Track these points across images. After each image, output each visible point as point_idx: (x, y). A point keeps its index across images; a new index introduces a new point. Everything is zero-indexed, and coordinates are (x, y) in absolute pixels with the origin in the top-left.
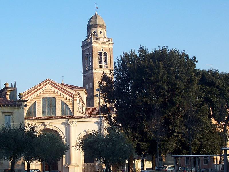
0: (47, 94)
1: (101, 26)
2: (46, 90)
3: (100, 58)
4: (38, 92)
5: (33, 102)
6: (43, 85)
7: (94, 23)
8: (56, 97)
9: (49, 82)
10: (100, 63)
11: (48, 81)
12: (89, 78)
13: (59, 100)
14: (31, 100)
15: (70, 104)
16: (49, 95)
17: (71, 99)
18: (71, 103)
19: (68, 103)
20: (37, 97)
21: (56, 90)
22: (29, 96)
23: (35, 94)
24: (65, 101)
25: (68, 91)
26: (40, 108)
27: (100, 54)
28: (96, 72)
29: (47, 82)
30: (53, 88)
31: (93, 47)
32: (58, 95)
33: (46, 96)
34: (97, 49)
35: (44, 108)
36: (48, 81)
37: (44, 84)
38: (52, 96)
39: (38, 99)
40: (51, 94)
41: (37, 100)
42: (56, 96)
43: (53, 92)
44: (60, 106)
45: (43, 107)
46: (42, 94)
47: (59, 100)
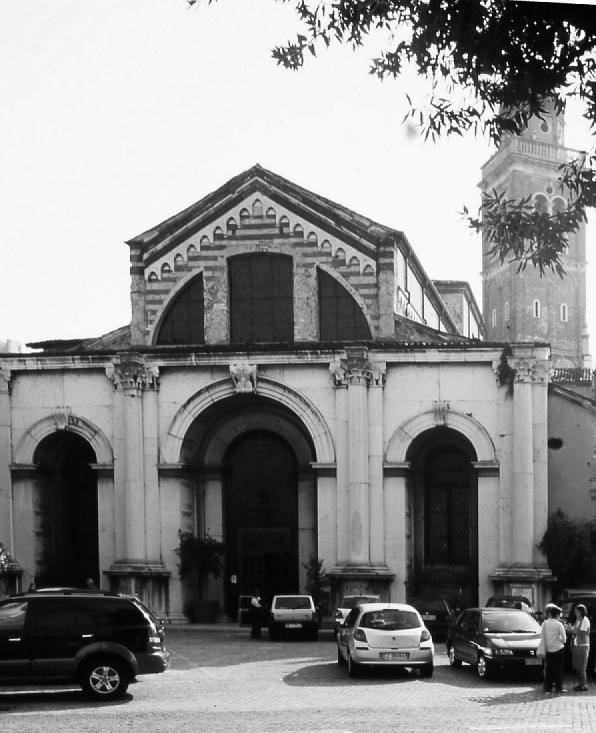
5: (187, 276)
12: (500, 289)
24: (334, 273)
30: (280, 211)
39: (211, 263)
41: (207, 268)
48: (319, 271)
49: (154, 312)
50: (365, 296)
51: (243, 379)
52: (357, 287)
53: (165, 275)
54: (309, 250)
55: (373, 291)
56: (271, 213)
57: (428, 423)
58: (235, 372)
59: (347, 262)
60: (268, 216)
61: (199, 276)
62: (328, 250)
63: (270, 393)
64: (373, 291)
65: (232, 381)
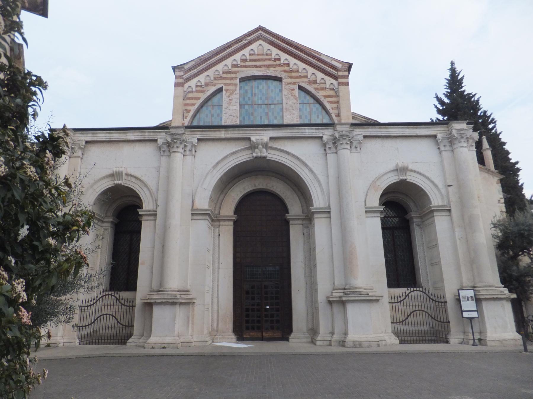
0: (256, 66)
4: (229, 62)
6: (244, 42)
8: (283, 75)
11: (260, 32)
13: (294, 84)
14: (207, 85)
16: (263, 69)
17: (329, 80)
21: (284, 57)
23: (220, 67)
26: (235, 108)
30: (275, 51)
33: (255, 72)
36: (260, 32)
39: (228, 82)
40: (268, 66)
41: (226, 85)
44: (295, 101)
45: (241, 106)
47: (294, 84)
49: (188, 111)
50: (331, 102)
51: (260, 146)
52: (326, 96)
53: (199, 88)
54: (294, 74)
55: (334, 99)
56: (269, 52)
57: (393, 179)
58: (255, 141)
59: (318, 81)
60: (267, 54)
62: (305, 75)
64: (334, 99)
65: (253, 147)
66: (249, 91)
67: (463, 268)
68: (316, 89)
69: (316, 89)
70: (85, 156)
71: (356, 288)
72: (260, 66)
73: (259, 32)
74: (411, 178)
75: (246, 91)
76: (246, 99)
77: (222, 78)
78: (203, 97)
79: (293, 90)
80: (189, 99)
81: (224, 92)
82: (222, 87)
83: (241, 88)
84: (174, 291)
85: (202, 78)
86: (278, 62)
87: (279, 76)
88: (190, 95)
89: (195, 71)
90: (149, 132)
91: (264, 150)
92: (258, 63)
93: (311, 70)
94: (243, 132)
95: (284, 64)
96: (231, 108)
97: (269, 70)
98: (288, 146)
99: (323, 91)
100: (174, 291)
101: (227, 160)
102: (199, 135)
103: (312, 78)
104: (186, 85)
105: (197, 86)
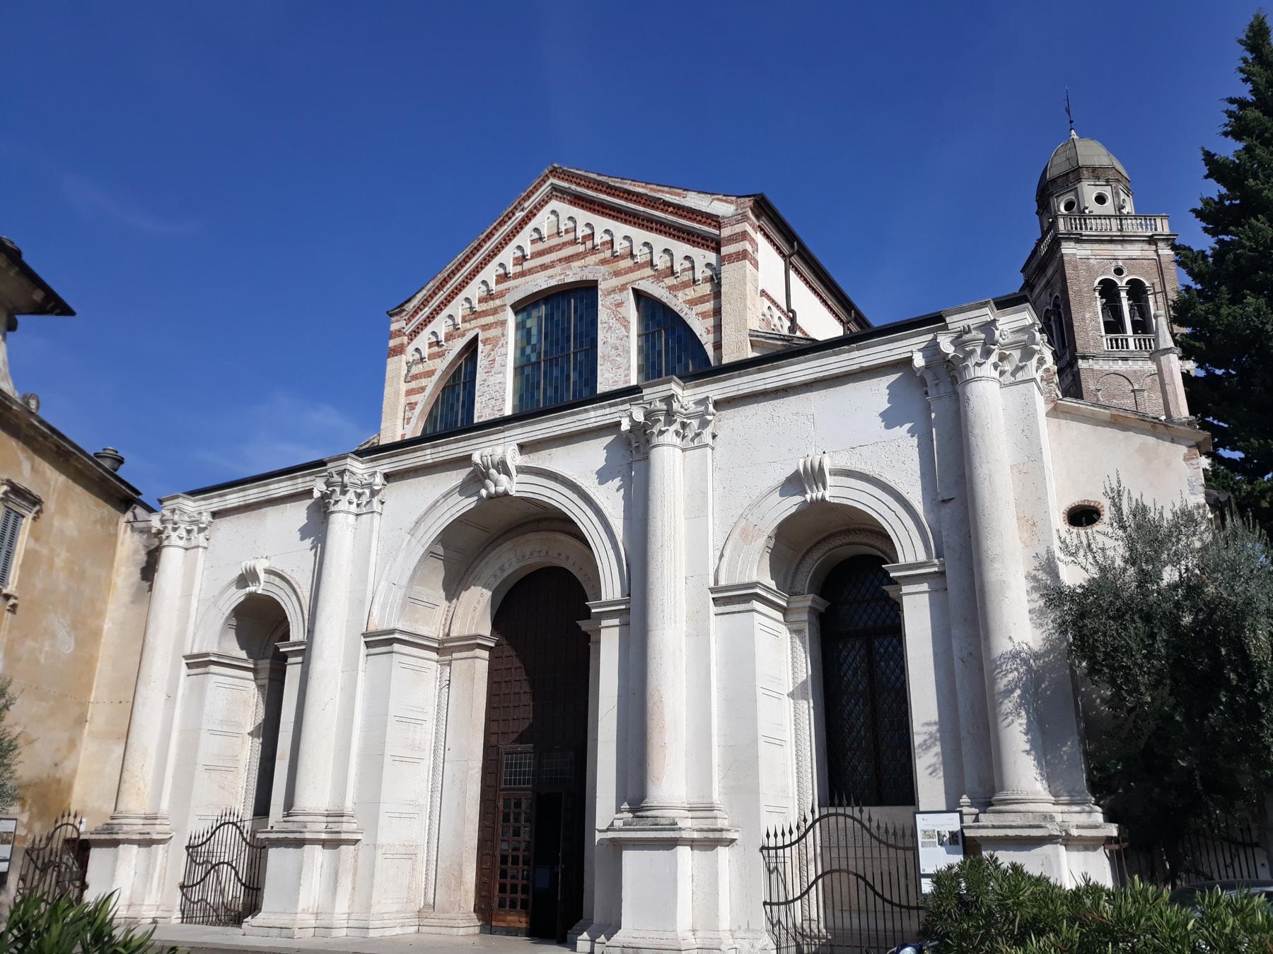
0: (544, 267)
1: (1096, 173)
2: (540, 246)
3: (1112, 308)
5: (459, 344)
6: (520, 215)
7: (1064, 168)
9: (556, 181)
10: (1114, 325)
13: (623, 288)
14: (449, 337)
15: (701, 300)
16: (558, 269)
17: (702, 257)
18: (706, 289)
19: (680, 294)
20: (484, 307)
22: (437, 311)
23: (474, 290)
24: (658, 291)
25: (680, 210)
27: (1108, 290)
28: (1096, 367)
29: (545, 188)
30: (583, 216)
31: (1065, 258)
32: (615, 257)
33: (541, 282)
34: (1089, 269)
35: (528, 370)
37: (528, 204)
38: (573, 274)
40: (569, 259)
41: (485, 327)
42: (603, 268)
43: (581, 248)
46: (516, 276)
47: (623, 288)
48: (639, 295)
51: (493, 471)
52: (692, 303)
53: (436, 349)
58: (479, 461)
61: (475, 339)
63: (548, 493)
65: (479, 477)
66: (534, 331)
67: (965, 748)
68: (671, 288)
69: (671, 288)
70: (212, 540)
71: (662, 808)
72: (552, 265)
73: (548, 183)
74: (834, 491)
75: (529, 330)
76: (528, 350)
77: (474, 314)
78: (441, 365)
79: (619, 305)
80: (415, 377)
81: (480, 346)
82: (475, 339)
83: (520, 326)
84: (316, 815)
85: (441, 326)
86: (589, 244)
87: (591, 277)
88: (416, 370)
89: (427, 311)
90: (303, 476)
91: (503, 477)
92: (546, 259)
93: (660, 242)
94: (466, 443)
95: (603, 244)
96: (491, 380)
97: (570, 268)
98: (556, 460)
99: (687, 291)
100: (316, 815)
101: (437, 513)
102: (387, 466)
103: (661, 262)
104: (410, 349)
105: (431, 345)
